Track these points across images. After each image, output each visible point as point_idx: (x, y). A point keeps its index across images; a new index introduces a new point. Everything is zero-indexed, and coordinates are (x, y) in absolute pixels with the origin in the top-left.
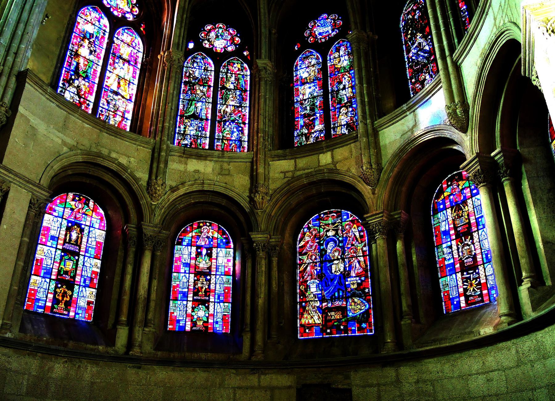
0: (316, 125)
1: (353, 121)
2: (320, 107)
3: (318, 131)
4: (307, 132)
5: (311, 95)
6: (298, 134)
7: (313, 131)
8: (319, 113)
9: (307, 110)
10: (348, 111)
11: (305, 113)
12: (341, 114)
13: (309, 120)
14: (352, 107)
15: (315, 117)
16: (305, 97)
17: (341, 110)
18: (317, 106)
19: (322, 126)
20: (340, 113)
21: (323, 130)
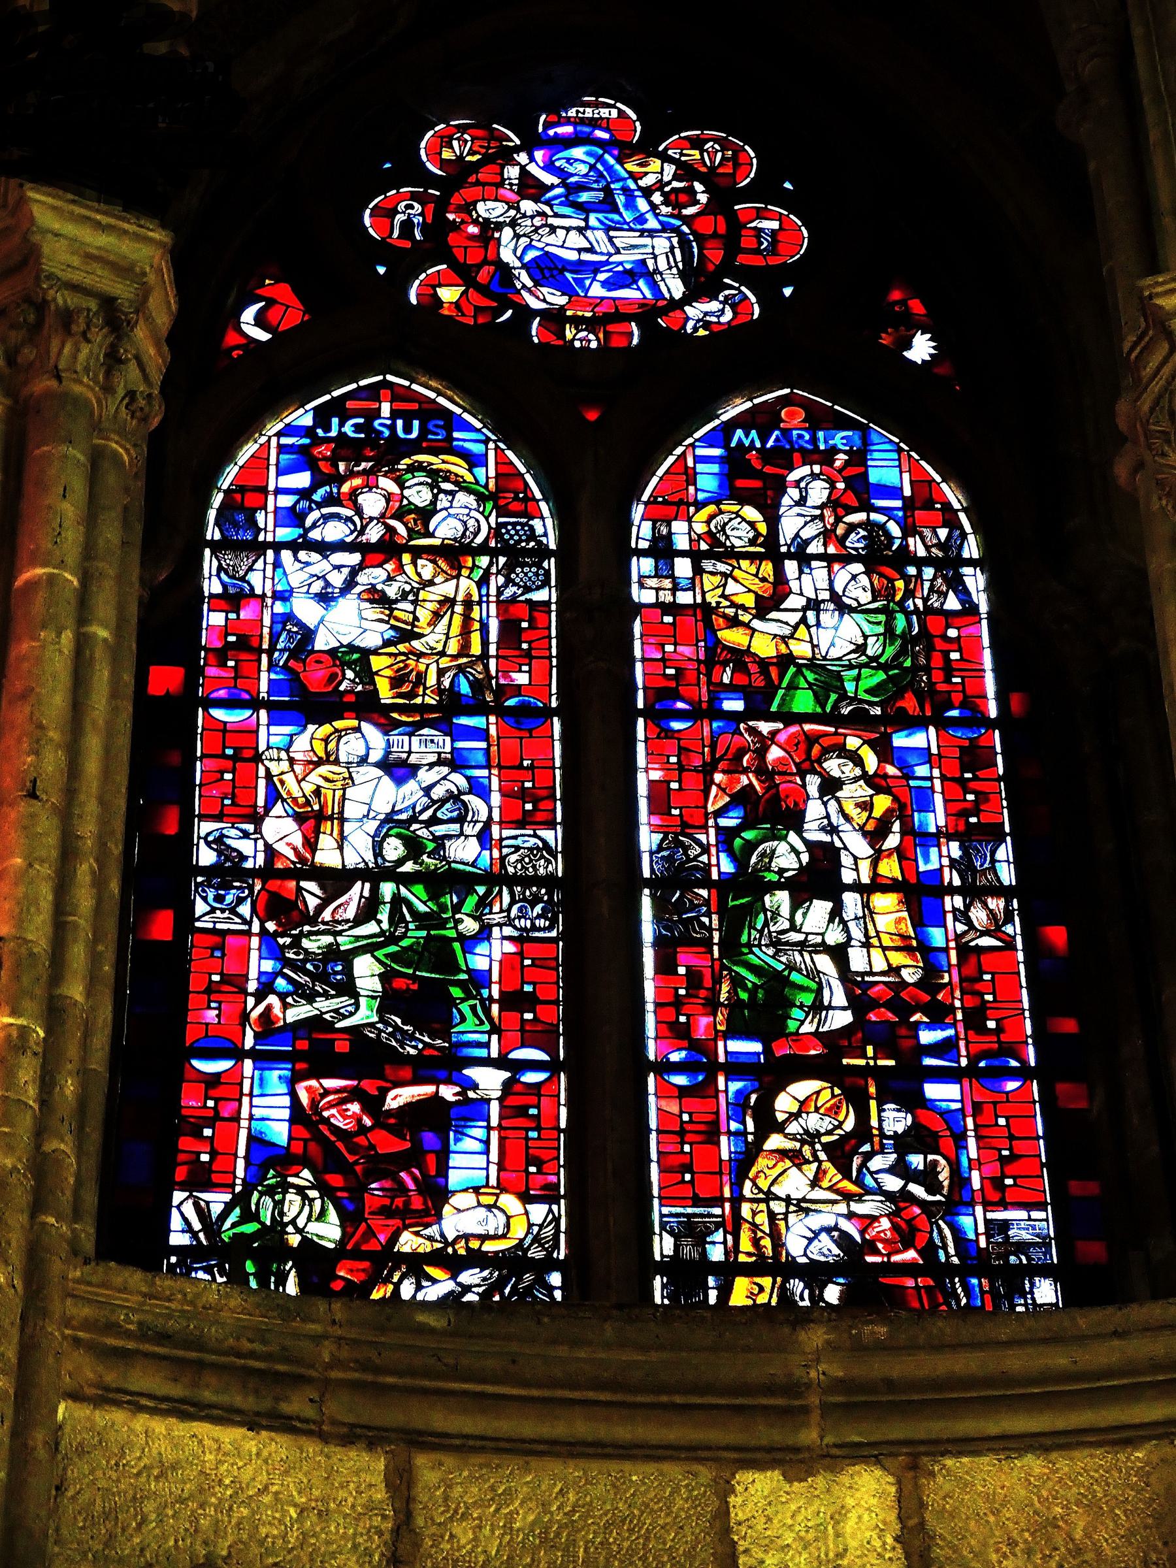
0: (455, 1179)
1: (929, 1251)
2: (512, 1001)
3: (477, 1259)
4: (329, 1231)
5: (414, 848)
6: (211, 1226)
7: (408, 1242)
8: (501, 1063)
9: (348, 988)
10: (862, 1131)
11: (316, 1022)
12: (775, 1141)
13: (373, 1104)
14: (913, 1101)
15: (448, 1093)
16: (326, 842)
17: (784, 1103)
18: (480, 979)
19: (538, 1212)
20: (768, 1124)
21: (551, 1264)
